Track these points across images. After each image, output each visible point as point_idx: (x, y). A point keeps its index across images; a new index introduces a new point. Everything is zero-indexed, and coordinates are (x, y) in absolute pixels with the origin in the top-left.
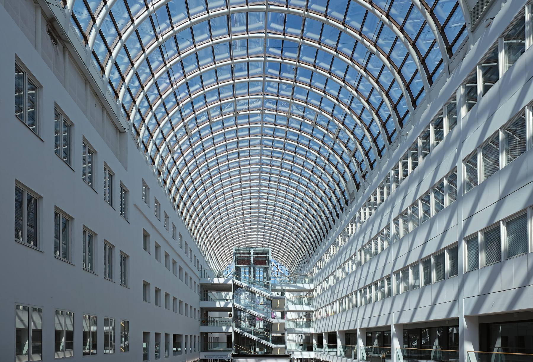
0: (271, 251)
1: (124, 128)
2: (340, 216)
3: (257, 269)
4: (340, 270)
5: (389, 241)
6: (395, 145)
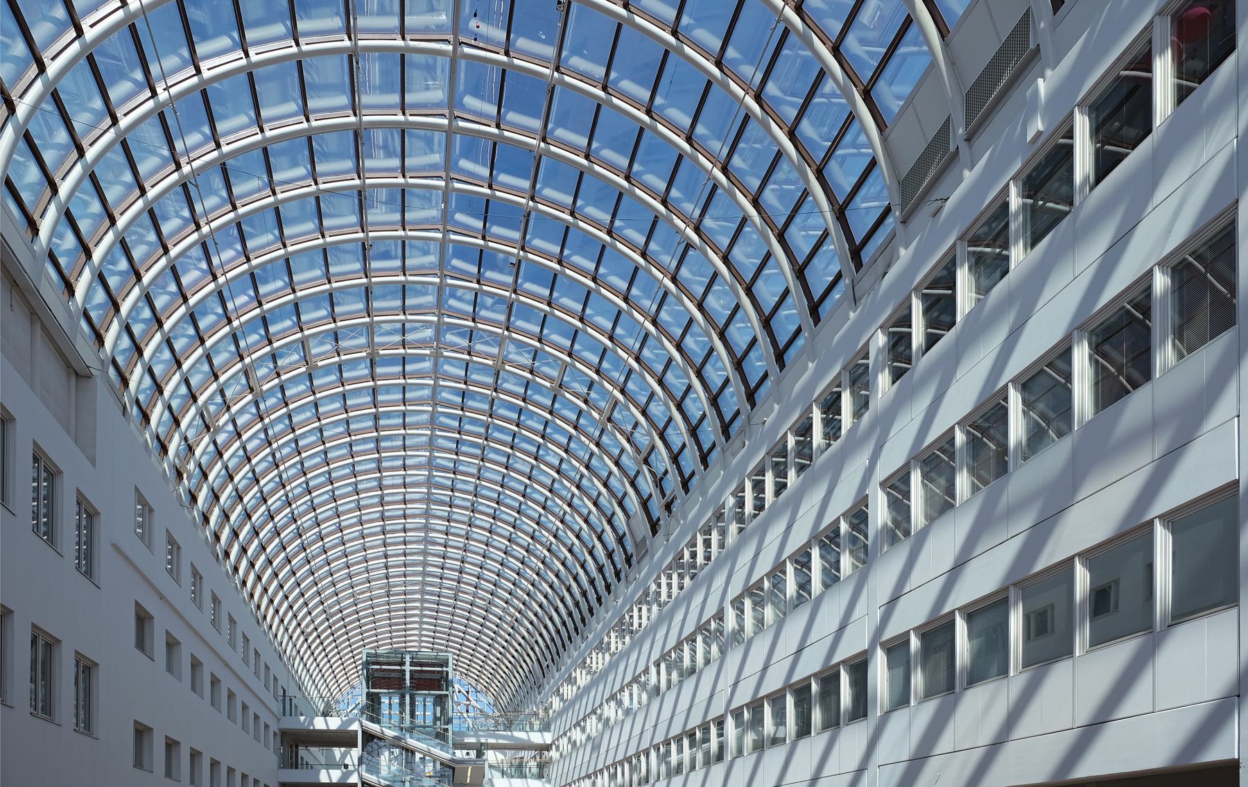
0: (454, 659)
1: (88, 367)
2: (612, 587)
3: (419, 700)
4: (613, 704)
5: (721, 644)
6: (738, 443)
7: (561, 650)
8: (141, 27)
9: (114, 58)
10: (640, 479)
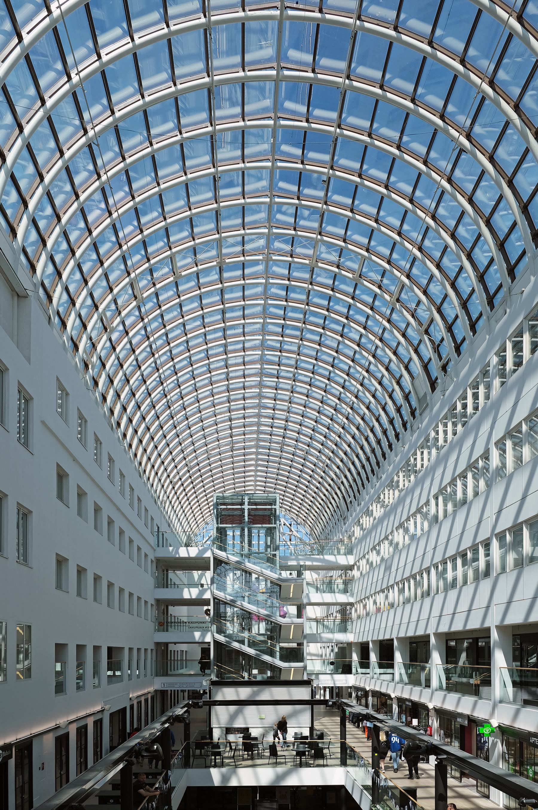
0: (280, 499)
1: (25, 289)
2: (400, 436)
3: (255, 532)
4: (401, 531)
5: (487, 479)
6: (500, 311)
7: (361, 488)
8: (61, 29)
9: (43, 55)
10: (422, 347)
